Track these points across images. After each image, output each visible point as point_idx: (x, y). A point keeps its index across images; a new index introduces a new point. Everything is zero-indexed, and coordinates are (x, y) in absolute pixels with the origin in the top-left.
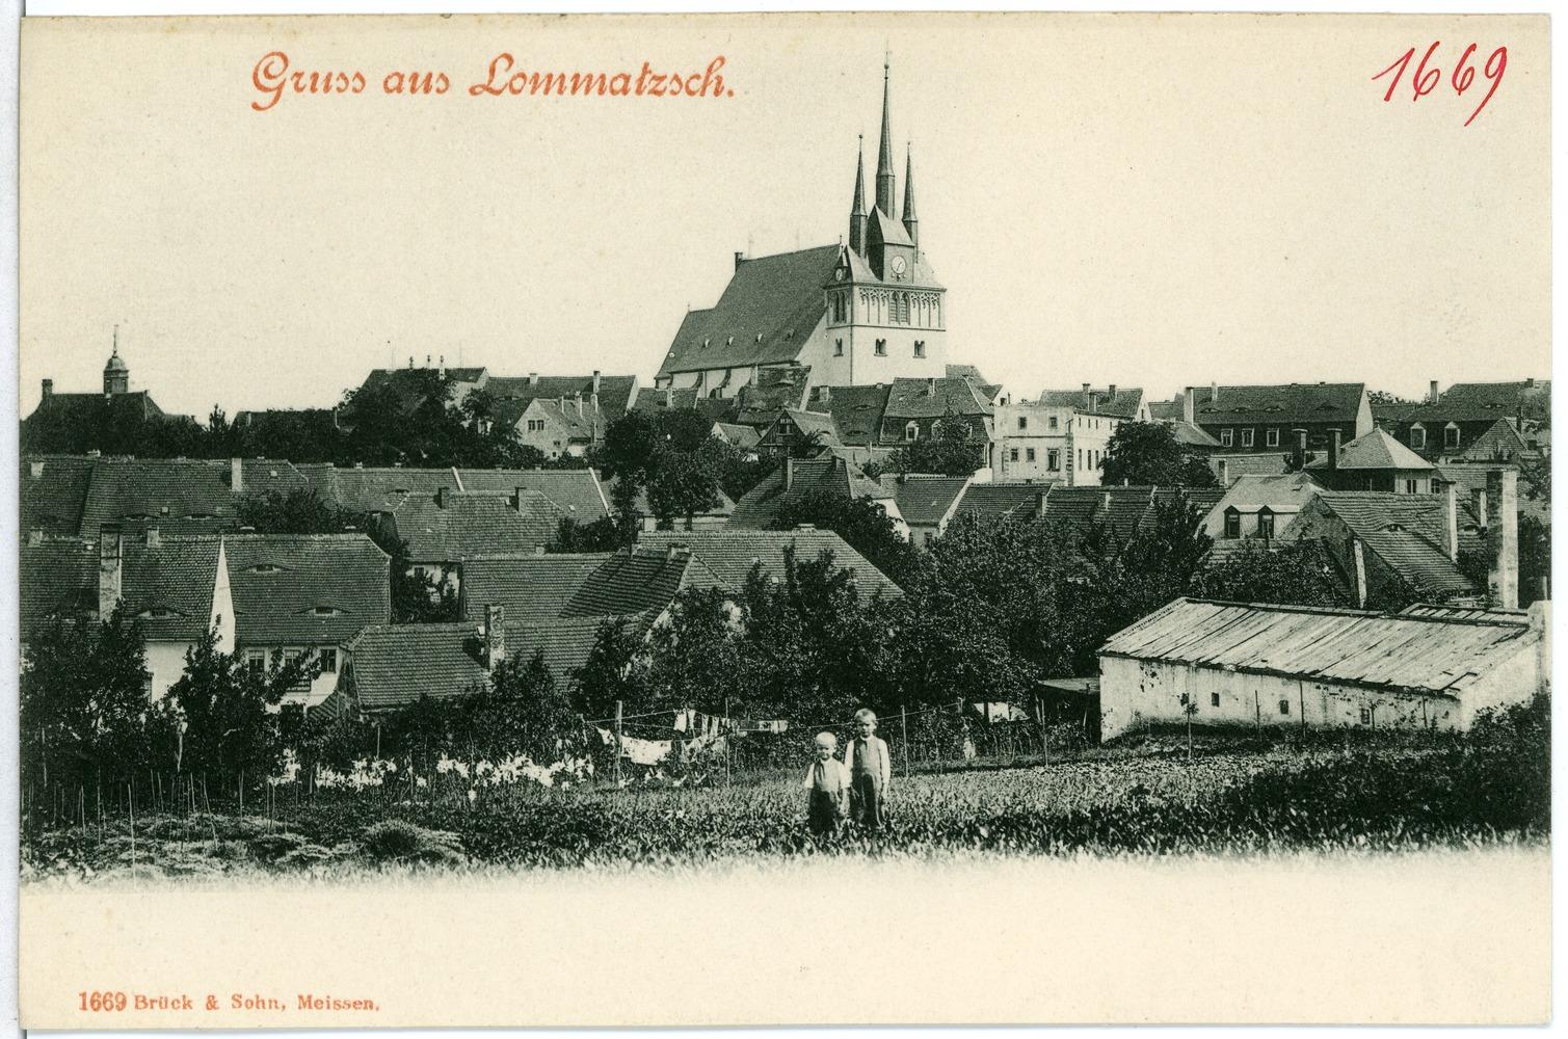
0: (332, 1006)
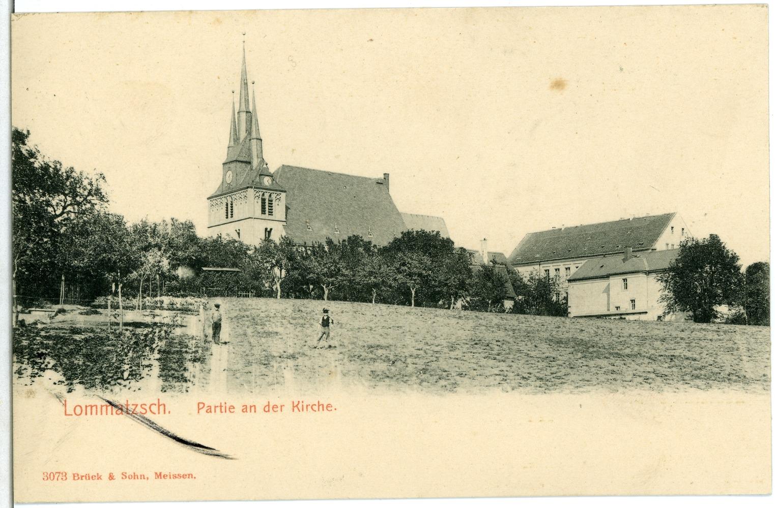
0: (172, 477)
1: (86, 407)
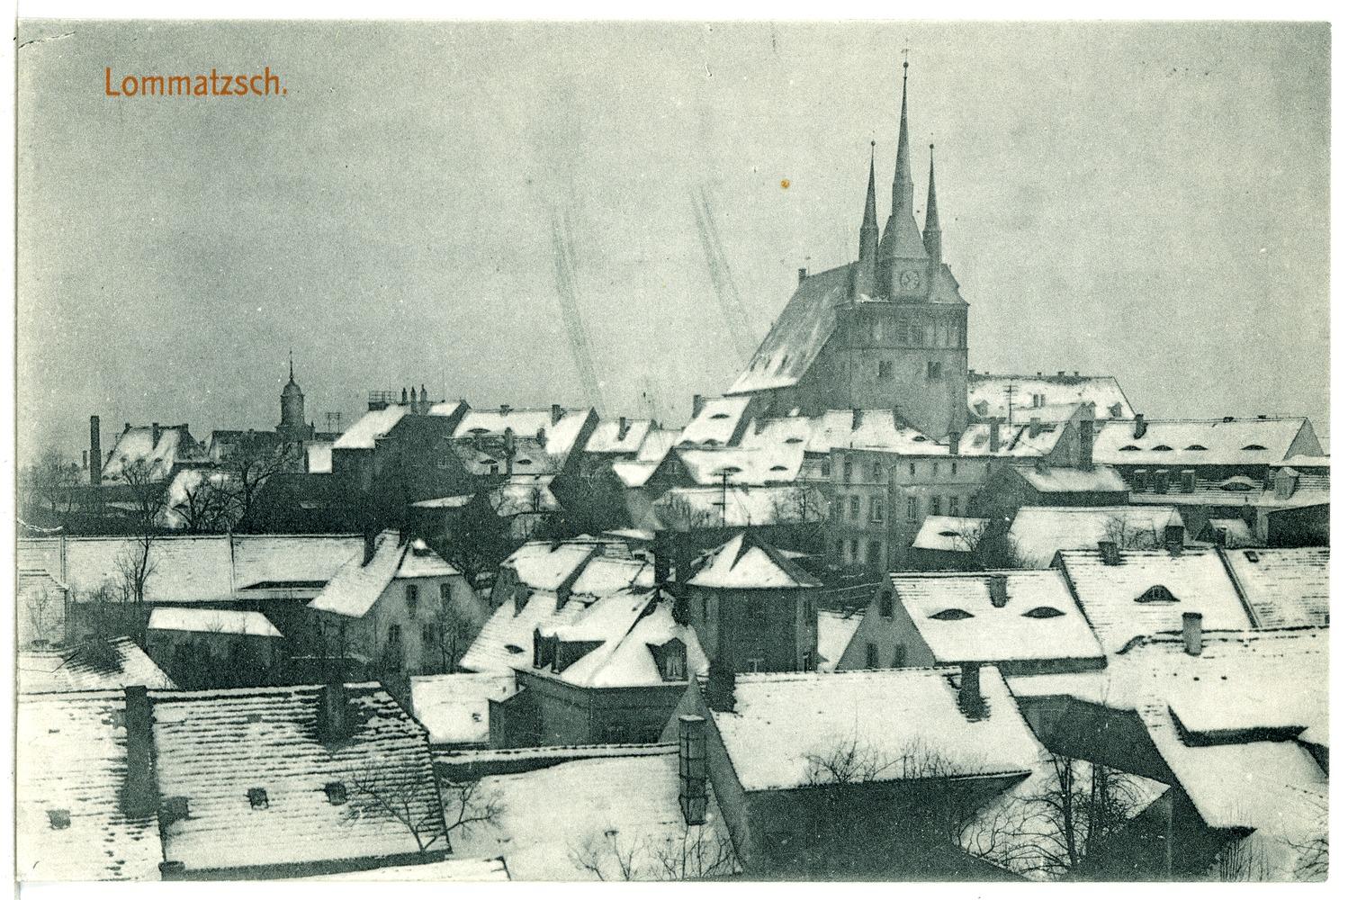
1: (171, 80)
